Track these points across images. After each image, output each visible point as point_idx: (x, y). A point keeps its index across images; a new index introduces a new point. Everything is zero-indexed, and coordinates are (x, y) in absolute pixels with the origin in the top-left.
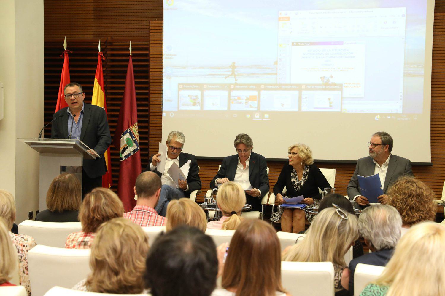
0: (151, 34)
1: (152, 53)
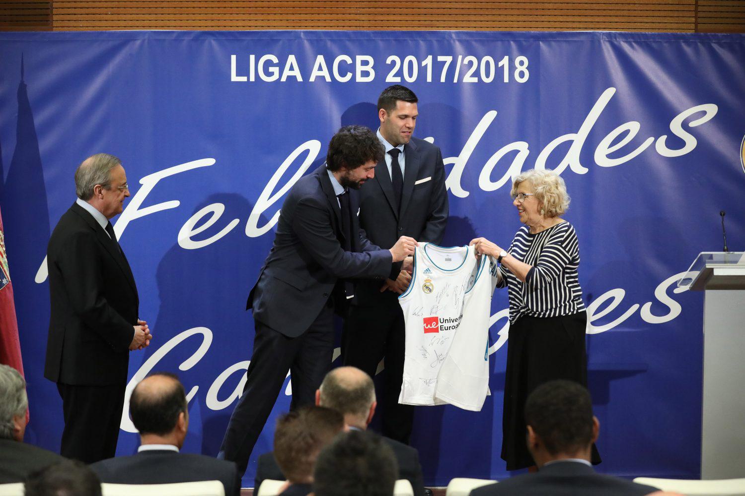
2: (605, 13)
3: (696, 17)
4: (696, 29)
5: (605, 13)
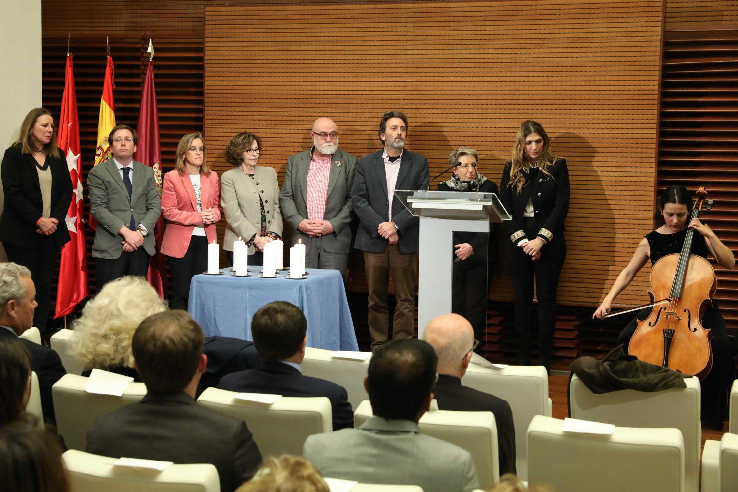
2: (588, 16)
4: (664, 27)
5: (588, 16)
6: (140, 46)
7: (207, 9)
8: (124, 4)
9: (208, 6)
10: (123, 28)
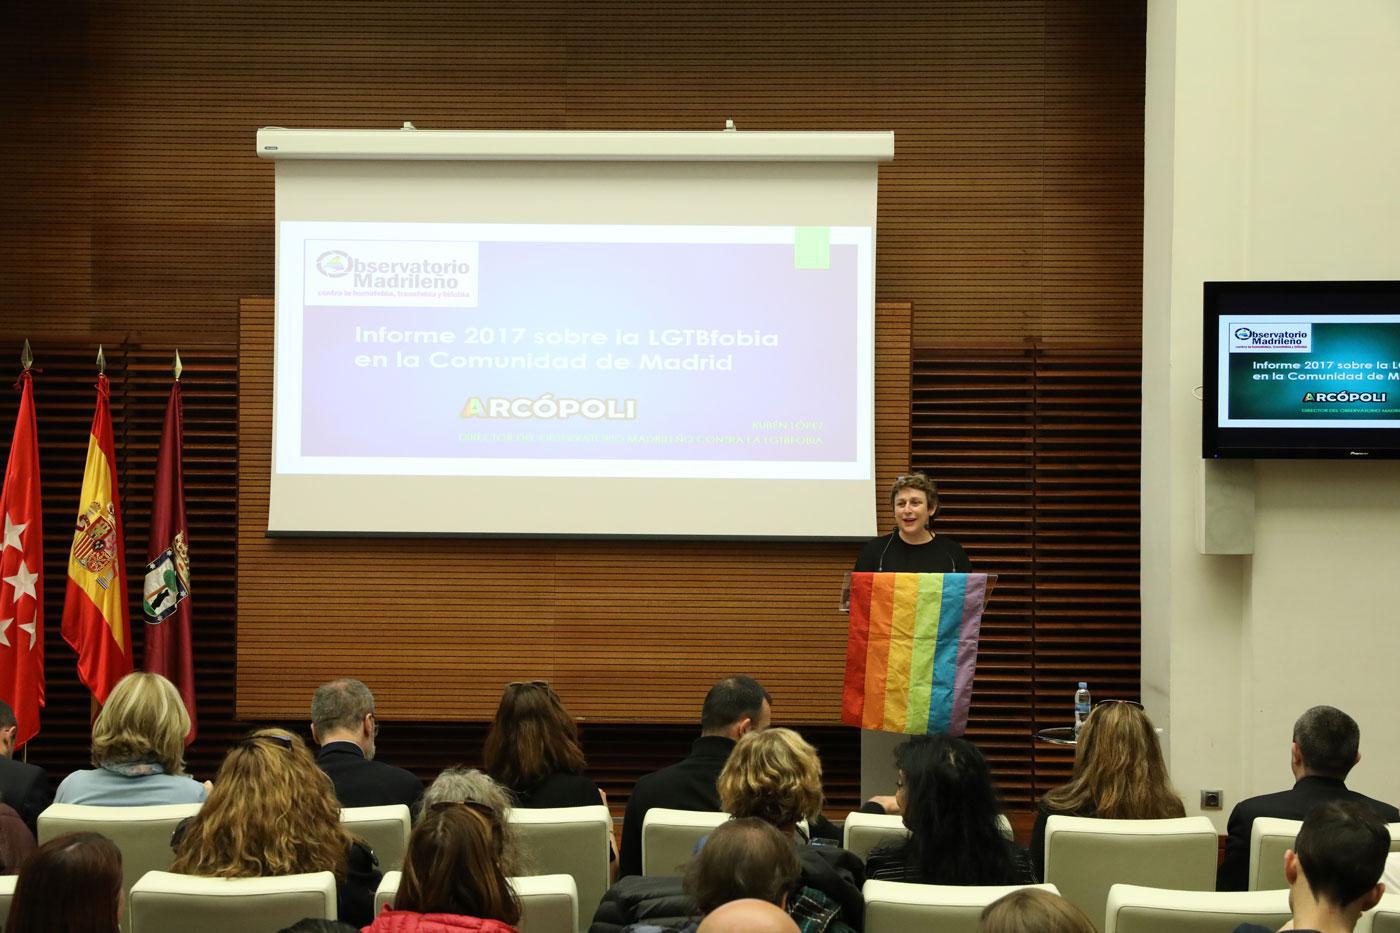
0: (242, 328)
1: (247, 372)
3: (911, 329)
4: (911, 342)
6: (121, 354)
7: (242, 301)
8: (88, 290)
9: (245, 295)
10: (88, 327)
